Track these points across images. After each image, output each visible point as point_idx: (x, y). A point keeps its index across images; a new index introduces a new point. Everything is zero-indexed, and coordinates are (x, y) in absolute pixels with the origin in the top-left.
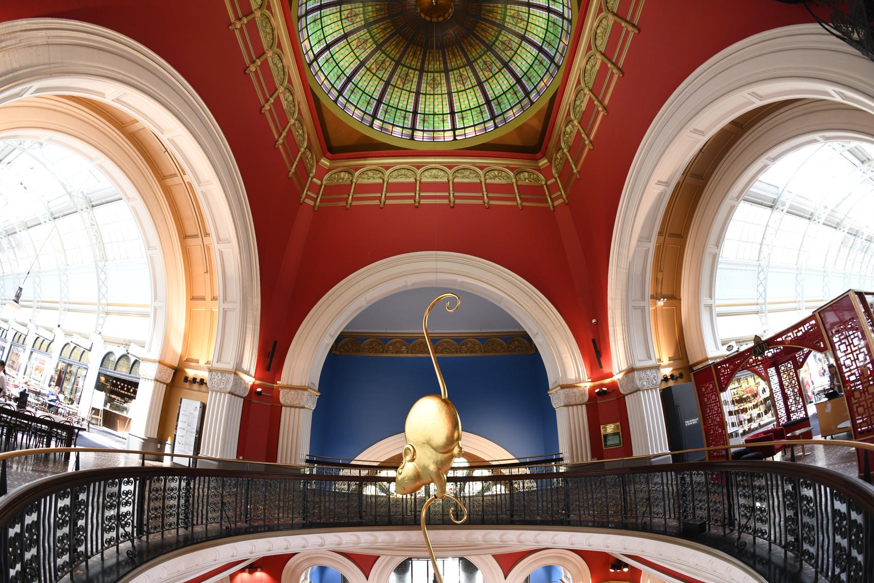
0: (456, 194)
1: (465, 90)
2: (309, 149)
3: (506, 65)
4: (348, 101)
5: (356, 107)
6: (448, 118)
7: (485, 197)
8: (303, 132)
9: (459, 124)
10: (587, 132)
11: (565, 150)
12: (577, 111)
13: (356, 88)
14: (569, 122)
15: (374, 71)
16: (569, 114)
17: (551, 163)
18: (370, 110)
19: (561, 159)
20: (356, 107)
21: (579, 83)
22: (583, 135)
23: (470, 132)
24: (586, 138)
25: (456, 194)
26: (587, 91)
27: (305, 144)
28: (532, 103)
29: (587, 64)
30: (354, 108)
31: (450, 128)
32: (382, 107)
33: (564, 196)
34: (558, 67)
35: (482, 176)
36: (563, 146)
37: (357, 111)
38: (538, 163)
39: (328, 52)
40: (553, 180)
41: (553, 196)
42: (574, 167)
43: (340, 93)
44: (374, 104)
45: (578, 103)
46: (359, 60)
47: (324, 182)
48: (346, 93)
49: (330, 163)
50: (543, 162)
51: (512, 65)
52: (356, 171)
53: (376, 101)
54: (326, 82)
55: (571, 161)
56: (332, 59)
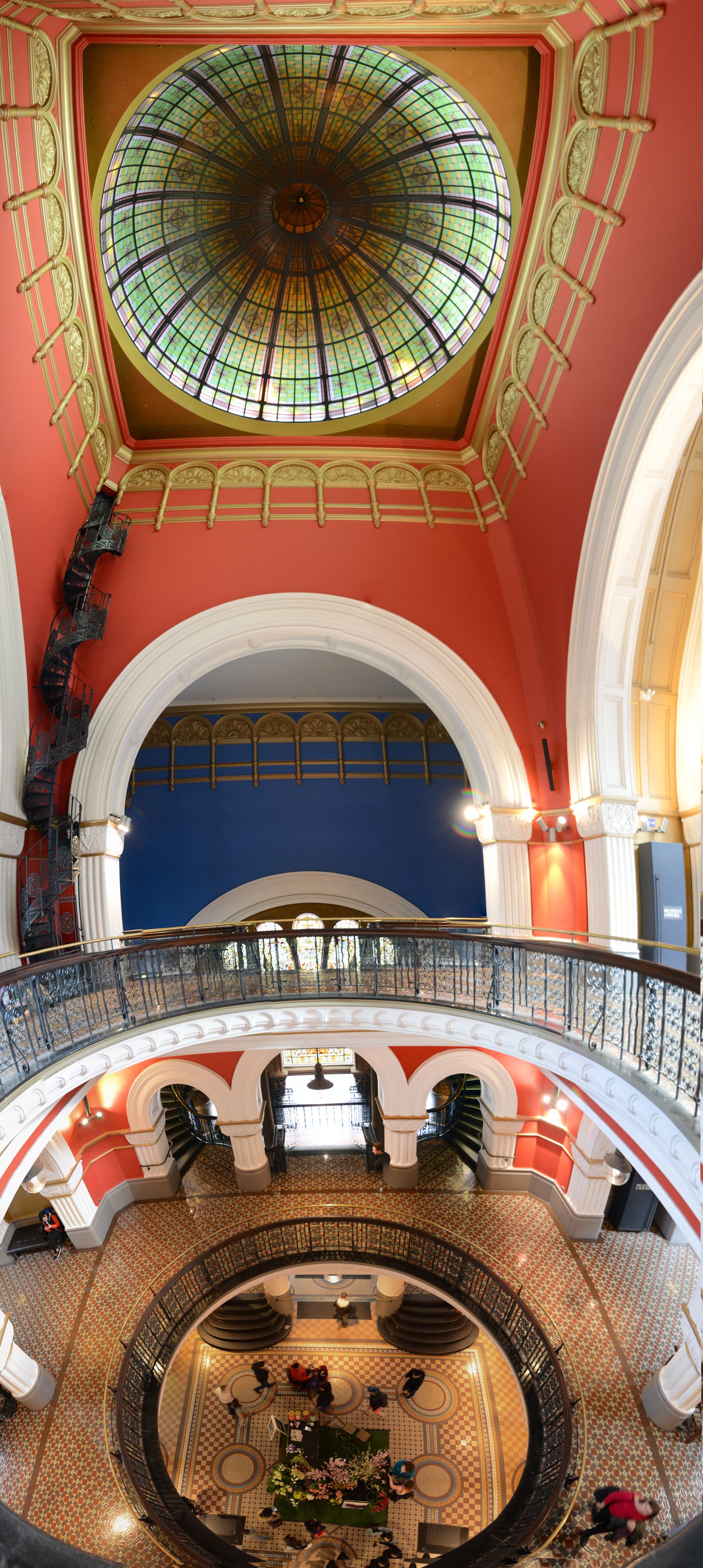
0: (328, 506)
1: (345, 340)
2: (101, 430)
3: (409, 299)
4: (164, 354)
5: (176, 365)
6: (318, 384)
7: (375, 510)
8: (94, 401)
9: (334, 395)
10: (538, 400)
11: (504, 434)
12: (521, 366)
13: (178, 335)
14: (508, 386)
15: (205, 309)
16: (508, 372)
17: (480, 454)
18: (198, 372)
19: (496, 448)
20: (176, 365)
21: (524, 319)
22: (532, 405)
23: (352, 408)
24: (535, 410)
25: (328, 506)
26: (537, 331)
27: (97, 422)
28: (449, 357)
29: (537, 287)
30: (173, 366)
31: (321, 401)
32: (216, 366)
33: (502, 509)
34: (492, 297)
35: (371, 477)
36: (499, 424)
37: (177, 372)
38: (460, 456)
39: (140, 272)
40: (484, 483)
41: (485, 509)
42: (516, 460)
43: (153, 341)
44: (204, 362)
45: (523, 352)
46: (185, 290)
47: (124, 487)
48: (162, 342)
49: (133, 454)
50: (469, 454)
51: (419, 298)
52: (172, 469)
53: (206, 357)
54: (133, 321)
55: (512, 449)
56: (144, 284)
